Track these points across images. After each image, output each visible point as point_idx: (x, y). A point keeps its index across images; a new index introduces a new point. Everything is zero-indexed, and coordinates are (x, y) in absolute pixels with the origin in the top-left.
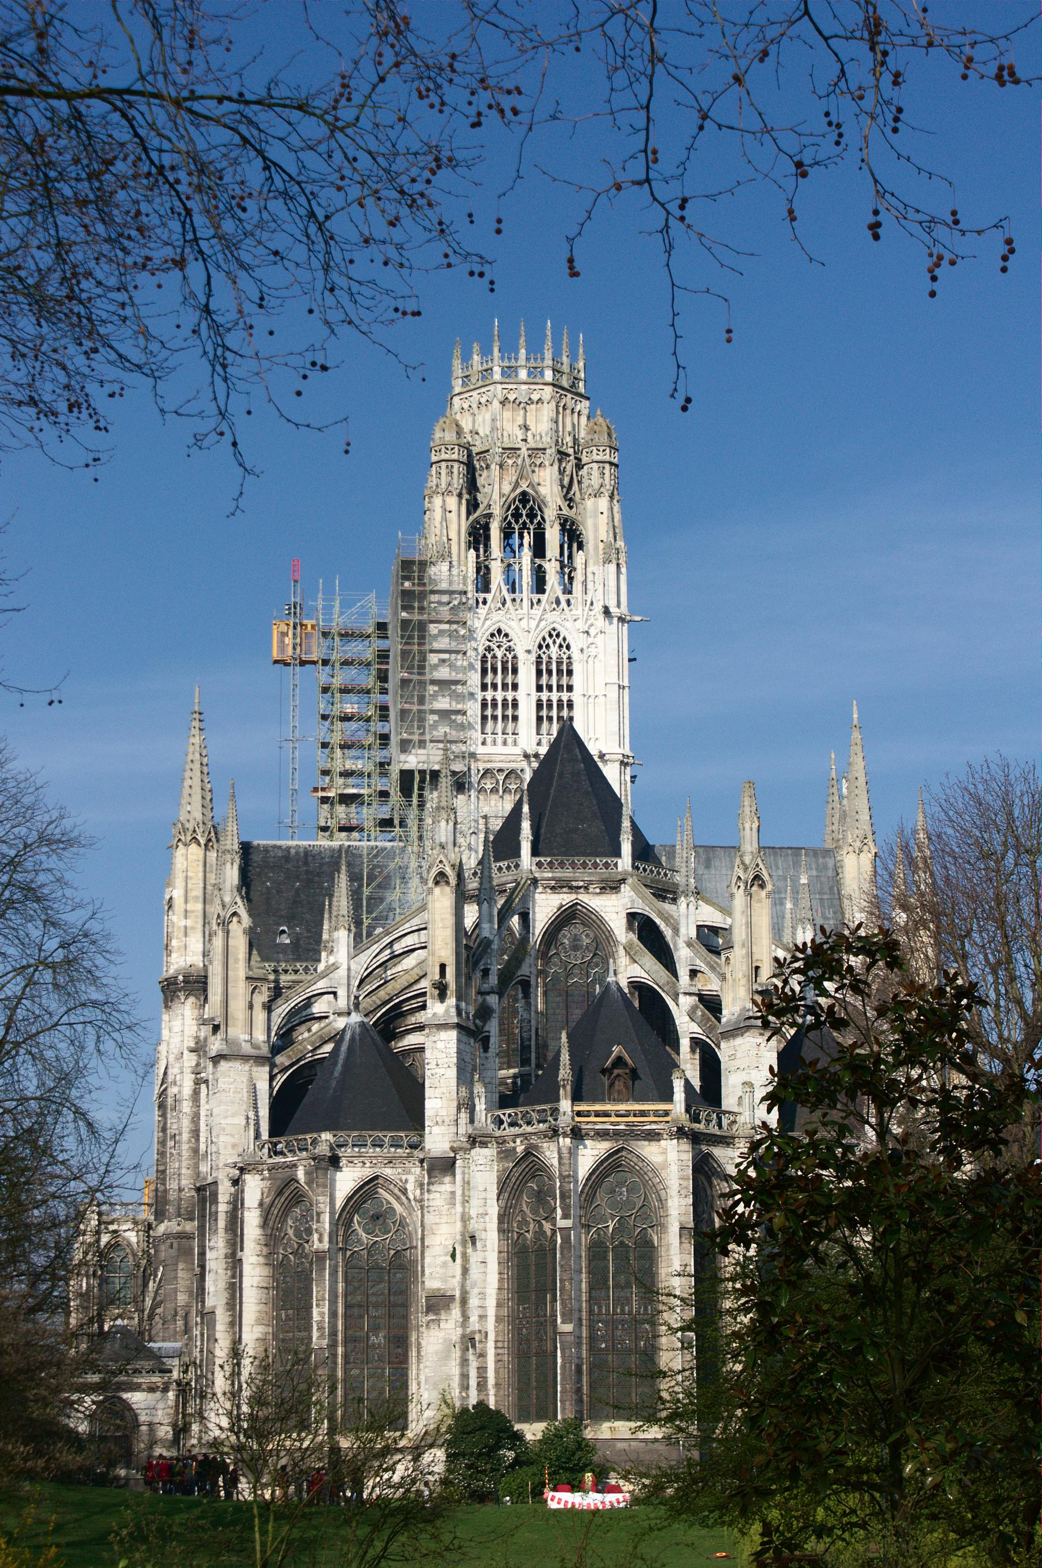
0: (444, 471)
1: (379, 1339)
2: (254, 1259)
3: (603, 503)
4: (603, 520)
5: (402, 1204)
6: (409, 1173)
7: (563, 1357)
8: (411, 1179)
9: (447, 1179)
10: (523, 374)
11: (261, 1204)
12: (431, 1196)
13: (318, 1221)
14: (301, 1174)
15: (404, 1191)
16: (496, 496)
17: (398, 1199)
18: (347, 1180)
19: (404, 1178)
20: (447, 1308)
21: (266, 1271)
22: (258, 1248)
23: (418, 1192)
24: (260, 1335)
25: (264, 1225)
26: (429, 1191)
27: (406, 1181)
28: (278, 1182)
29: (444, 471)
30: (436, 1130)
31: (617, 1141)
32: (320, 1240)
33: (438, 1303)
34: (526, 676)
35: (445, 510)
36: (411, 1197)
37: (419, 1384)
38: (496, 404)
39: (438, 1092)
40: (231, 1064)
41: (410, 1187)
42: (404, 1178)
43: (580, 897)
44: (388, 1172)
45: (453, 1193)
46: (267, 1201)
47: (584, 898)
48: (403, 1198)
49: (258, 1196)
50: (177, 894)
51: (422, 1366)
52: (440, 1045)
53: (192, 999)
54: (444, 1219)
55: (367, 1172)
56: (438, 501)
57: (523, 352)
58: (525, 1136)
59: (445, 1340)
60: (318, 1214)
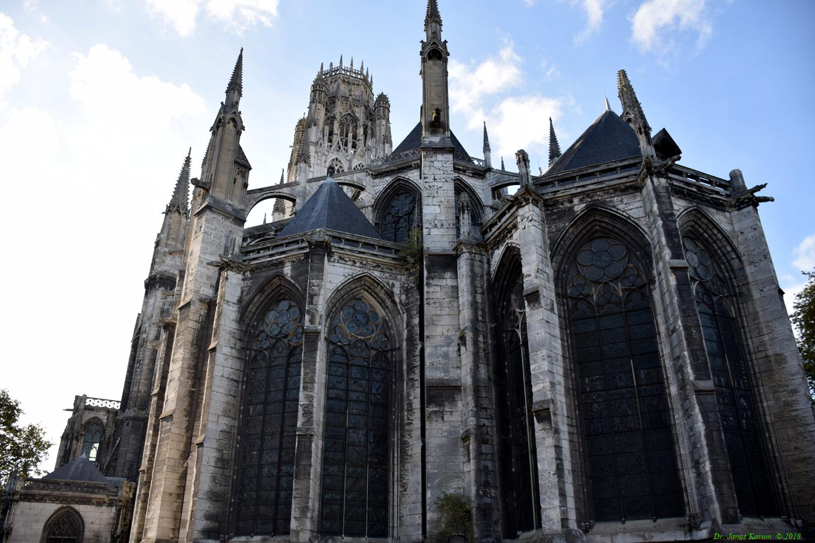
1: (357, 437)
2: (227, 350)
5: (385, 307)
6: (396, 279)
7: (706, 422)
8: (397, 284)
9: (448, 275)
11: (240, 301)
12: (431, 289)
13: (311, 303)
14: (287, 270)
15: (390, 295)
17: (382, 303)
18: (335, 274)
19: (391, 282)
20: (453, 401)
21: (237, 365)
22: (233, 341)
23: (403, 297)
24: (225, 427)
25: (240, 320)
26: (428, 284)
27: (393, 285)
28: (261, 280)
30: (434, 232)
31: (691, 202)
32: (312, 321)
33: (440, 394)
36: (397, 300)
37: (404, 486)
39: (435, 201)
40: (214, 216)
41: (396, 290)
42: (391, 282)
43: (461, 176)
44: (376, 274)
45: (456, 289)
46: (247, 298)
47: (464, 178)
48: (388, 302)
49: (238, 293)
51: (408, 466)
54: (446, 311)
55: (357, 271)
58: (584, 195)
59: (450, 433)
60: (312, 297)
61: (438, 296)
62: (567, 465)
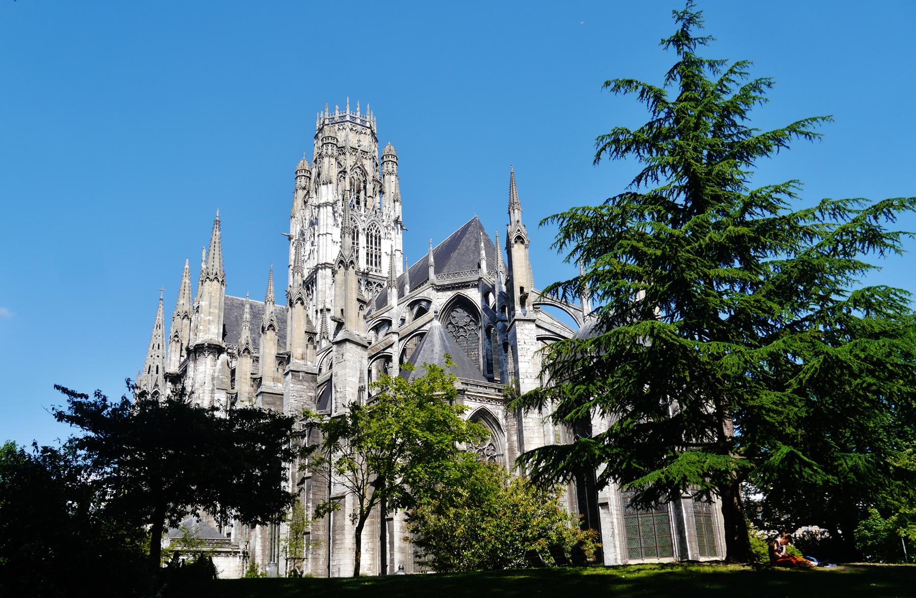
0: (330, 148)
3: (393, 178)
4: (393, 184)
8: (500, 413)
10: (358, 121)
16: (348, 165)
29: (330, 148)
30: (526, 381)
34: (362, 239)
35: (330, 164)
38: (348, 129)
44: (488, 406)
50: (204, 303)
52: (526, 332)
53: (211, 356)
54: (536, 435)
56: (326, 160)
57: (358, 113)
61: (531, 424)
62: (616, 531)
